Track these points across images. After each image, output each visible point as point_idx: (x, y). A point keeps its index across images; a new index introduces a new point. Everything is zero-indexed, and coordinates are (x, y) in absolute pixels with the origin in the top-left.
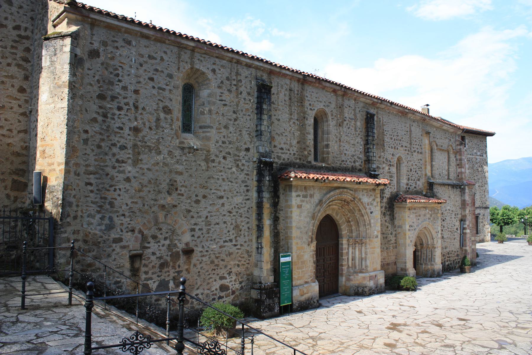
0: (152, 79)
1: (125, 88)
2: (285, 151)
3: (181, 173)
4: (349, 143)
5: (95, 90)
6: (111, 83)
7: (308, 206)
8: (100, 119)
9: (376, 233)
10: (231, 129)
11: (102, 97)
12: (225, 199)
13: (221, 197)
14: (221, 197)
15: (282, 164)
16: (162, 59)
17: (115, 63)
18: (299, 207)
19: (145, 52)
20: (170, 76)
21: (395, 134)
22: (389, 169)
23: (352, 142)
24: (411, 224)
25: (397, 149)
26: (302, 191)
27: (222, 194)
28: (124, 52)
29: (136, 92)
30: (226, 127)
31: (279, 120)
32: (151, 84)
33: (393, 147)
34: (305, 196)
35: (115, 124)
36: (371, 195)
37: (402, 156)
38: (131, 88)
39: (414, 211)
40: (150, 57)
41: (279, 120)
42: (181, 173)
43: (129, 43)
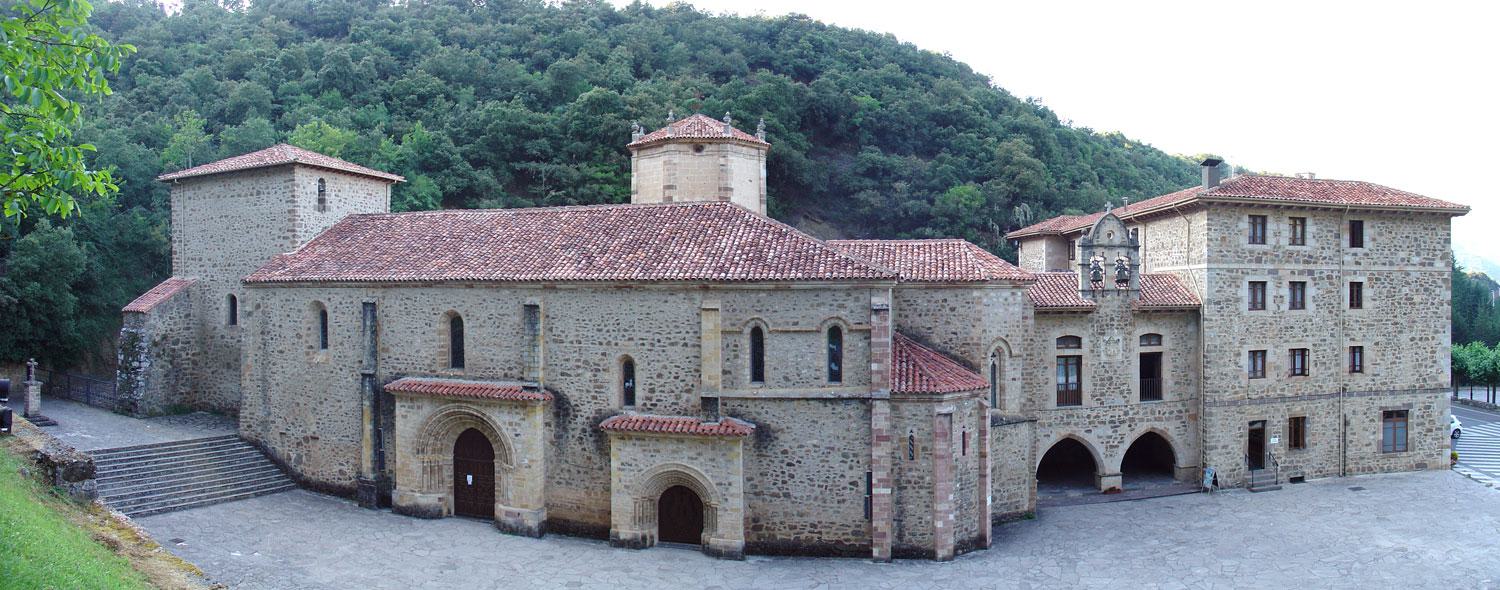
0: (288, 316)
1: (274, 325)
2: (401, 361)
3: (309, 381)
4: (500, 346)
5: (259, 330)
6: (267, 323)
7: (415, 417)
8: (262, 346)
9: (526, 461)
10: (346, 346)
11: (262, 333)
12: (342, 403)
13: (339, 401)
14: (339, 401)
15: (398, 374)
16: (294, 300)
17: (269, 309)
18: (405, 417)
19: (283, 297)
20: (300, 311)
21: (612, 322)
22: (595, 376)
23: (505, 344)
24: (624, 460)
25: (616, 344)
26: (406, 401)
27: (340, 398)
28: (273, 301)
29: (280, 326)
30: (341, 344)
31: (393, 331)
32: (289, 319)
33: (605, 342)
34: (412, 408)
35: (270, 349)
36: (517, 413)
37: (632, 355)
38: (277, 324)
39: (637, 443)
40: (287, 300)
41: (393, 331)
42: (309, 381)
43: (275, 294)
